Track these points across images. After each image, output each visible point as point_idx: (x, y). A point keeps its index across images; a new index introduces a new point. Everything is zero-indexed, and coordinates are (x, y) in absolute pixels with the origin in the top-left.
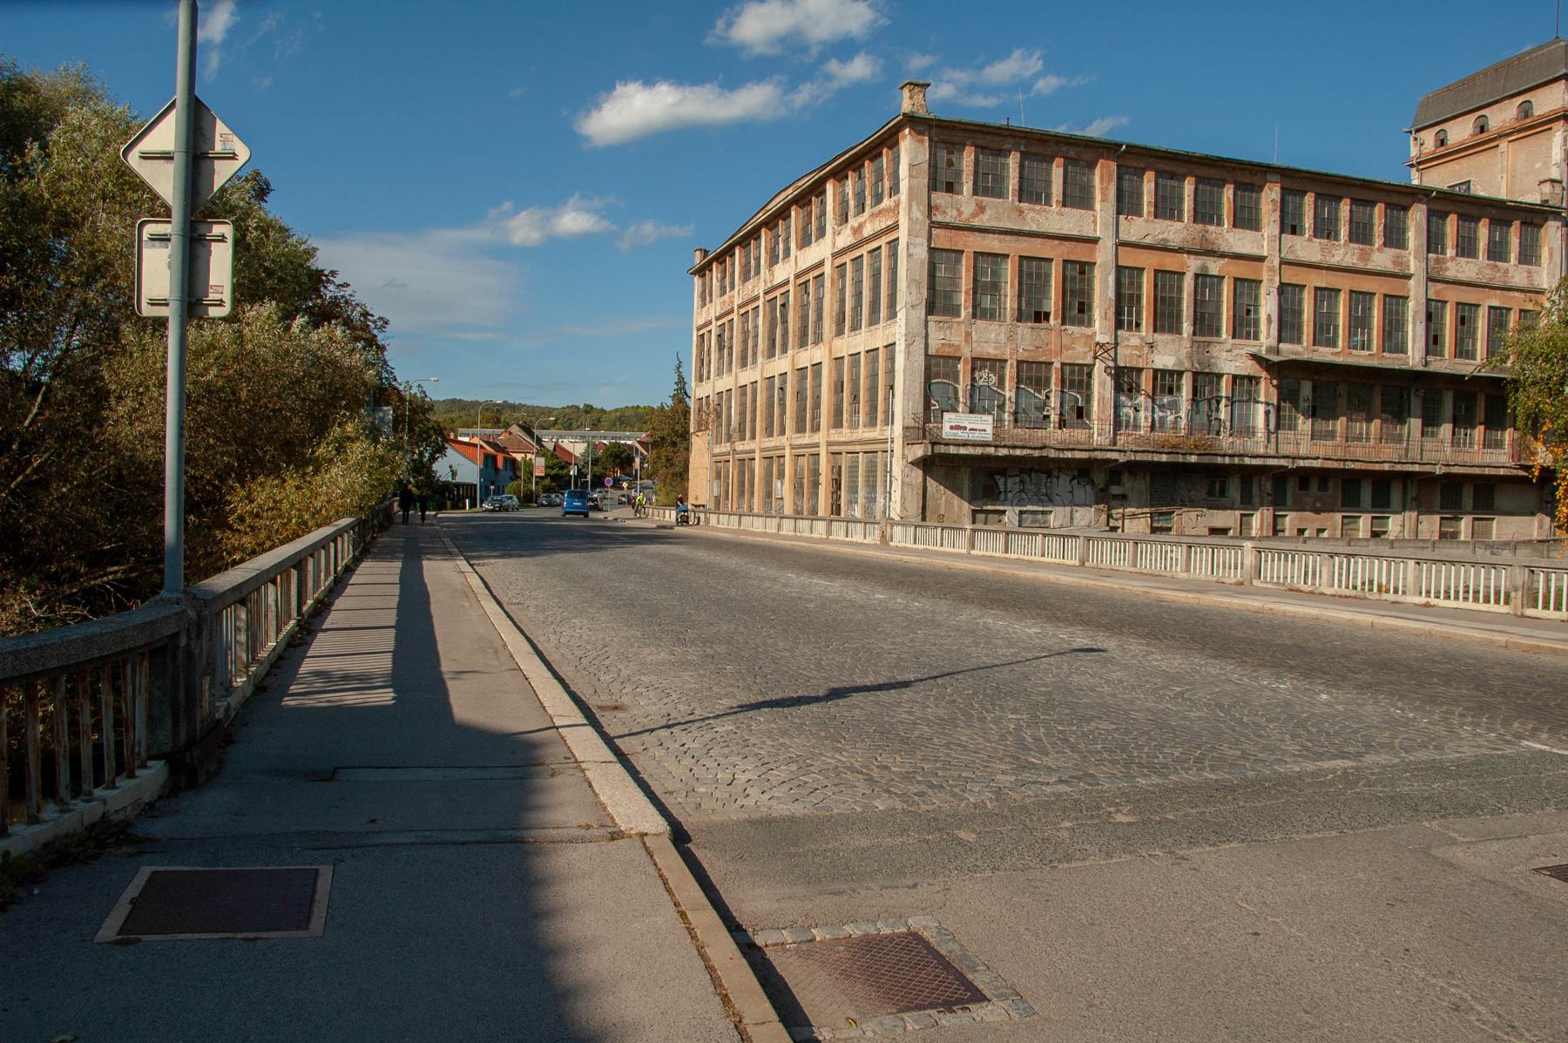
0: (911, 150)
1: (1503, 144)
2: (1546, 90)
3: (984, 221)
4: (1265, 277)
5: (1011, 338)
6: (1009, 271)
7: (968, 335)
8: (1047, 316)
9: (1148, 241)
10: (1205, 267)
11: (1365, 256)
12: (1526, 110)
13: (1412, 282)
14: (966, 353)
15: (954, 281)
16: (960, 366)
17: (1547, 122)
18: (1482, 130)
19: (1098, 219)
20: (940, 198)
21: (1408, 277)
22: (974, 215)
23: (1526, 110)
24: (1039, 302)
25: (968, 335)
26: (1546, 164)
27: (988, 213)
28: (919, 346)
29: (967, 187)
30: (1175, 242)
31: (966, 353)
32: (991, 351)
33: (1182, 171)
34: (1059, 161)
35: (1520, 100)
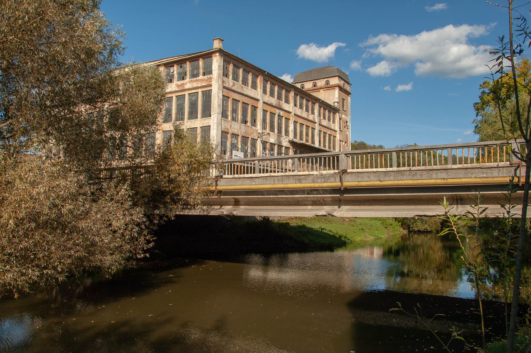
0: (217, 62)
1: (322, 91)
2: (333, 78)
3: (234, 88)
4: (291, 118)
5: (240, 128)
6: (240, 105)
7: (231, 125)
8: (247, 122)
9: (269, 102)
10: (279, 113)
11: (308, 116)
12: (327, 83)
13: (316, 124)
14: (230, 132)
15: (227, 106)
16: (229, 136)
17: (333, 87)
18: (315, 86)
19: (258, 93)
20: (225, 79)
21: (315, 123)
22: (232, 86)
23: (327, 83)
24: (246, 118)
25: (231, 125)
26: (334, 98)
27: (236, 86)
28: (220, 128)
29: (231, 77)
30: (274, 104)
31: (230, 132)
32: (236, 132)
33: (275, 83)
34: (251, 73)
35: (326, 80)
